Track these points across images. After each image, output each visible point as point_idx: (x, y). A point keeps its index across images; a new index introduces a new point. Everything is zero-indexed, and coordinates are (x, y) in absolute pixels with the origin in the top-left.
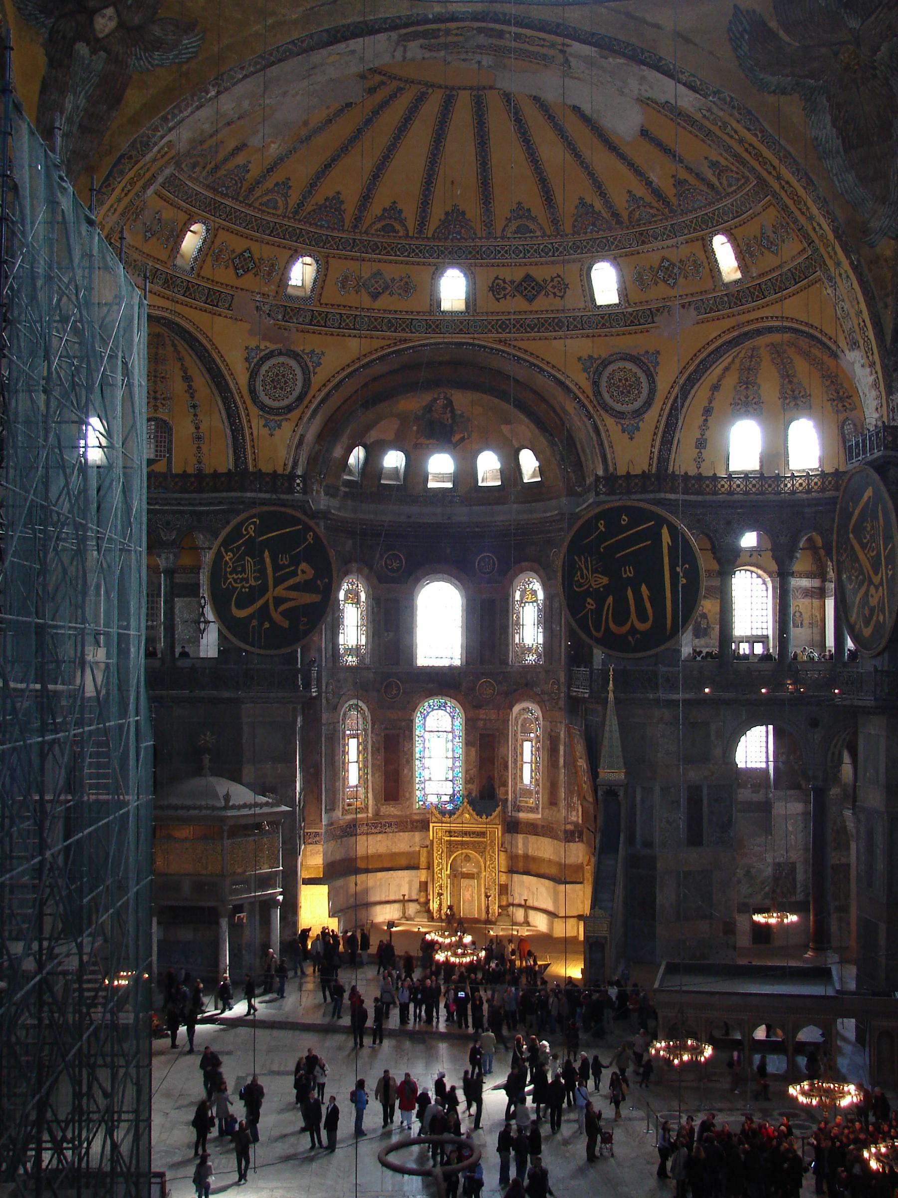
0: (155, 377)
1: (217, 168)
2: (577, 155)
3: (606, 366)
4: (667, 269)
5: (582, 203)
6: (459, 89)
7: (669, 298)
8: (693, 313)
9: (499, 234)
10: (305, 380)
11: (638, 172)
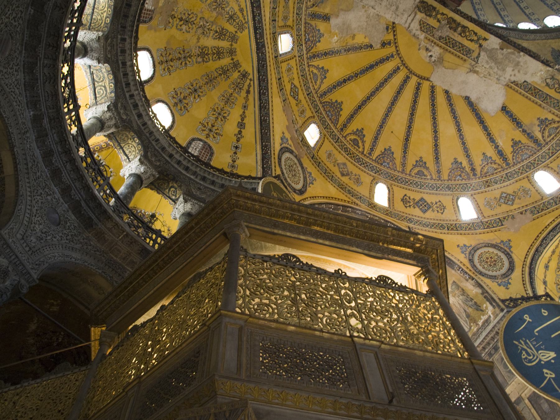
0: (219, 114)
1: (314, 16)
2: (459, 130)
3: (475, 251)
4: (506, 197)
5: (456, 161)
6: (414, 74)
7: (511, 211)
8: (528, 214)
9: (408, 172)
10: (304, 185)
11: (492, 140)
